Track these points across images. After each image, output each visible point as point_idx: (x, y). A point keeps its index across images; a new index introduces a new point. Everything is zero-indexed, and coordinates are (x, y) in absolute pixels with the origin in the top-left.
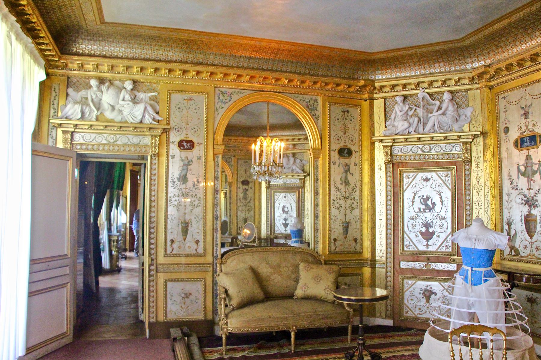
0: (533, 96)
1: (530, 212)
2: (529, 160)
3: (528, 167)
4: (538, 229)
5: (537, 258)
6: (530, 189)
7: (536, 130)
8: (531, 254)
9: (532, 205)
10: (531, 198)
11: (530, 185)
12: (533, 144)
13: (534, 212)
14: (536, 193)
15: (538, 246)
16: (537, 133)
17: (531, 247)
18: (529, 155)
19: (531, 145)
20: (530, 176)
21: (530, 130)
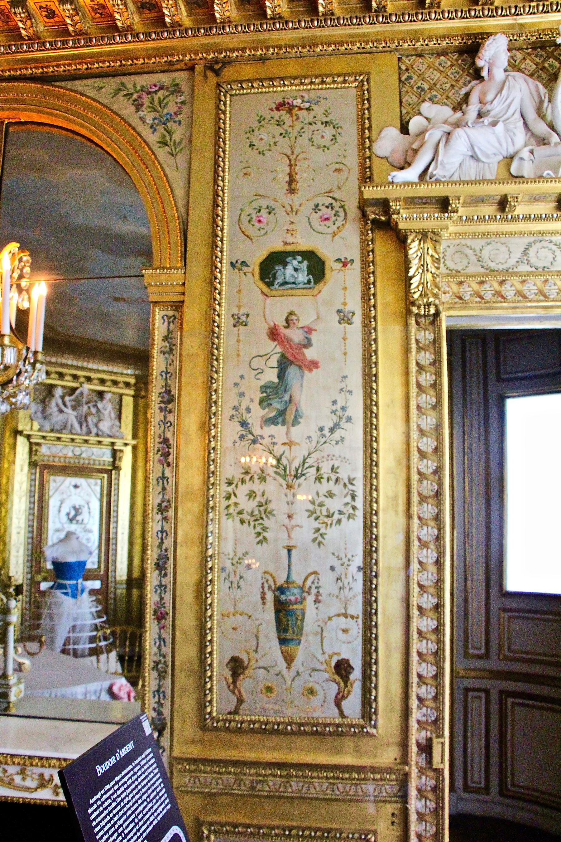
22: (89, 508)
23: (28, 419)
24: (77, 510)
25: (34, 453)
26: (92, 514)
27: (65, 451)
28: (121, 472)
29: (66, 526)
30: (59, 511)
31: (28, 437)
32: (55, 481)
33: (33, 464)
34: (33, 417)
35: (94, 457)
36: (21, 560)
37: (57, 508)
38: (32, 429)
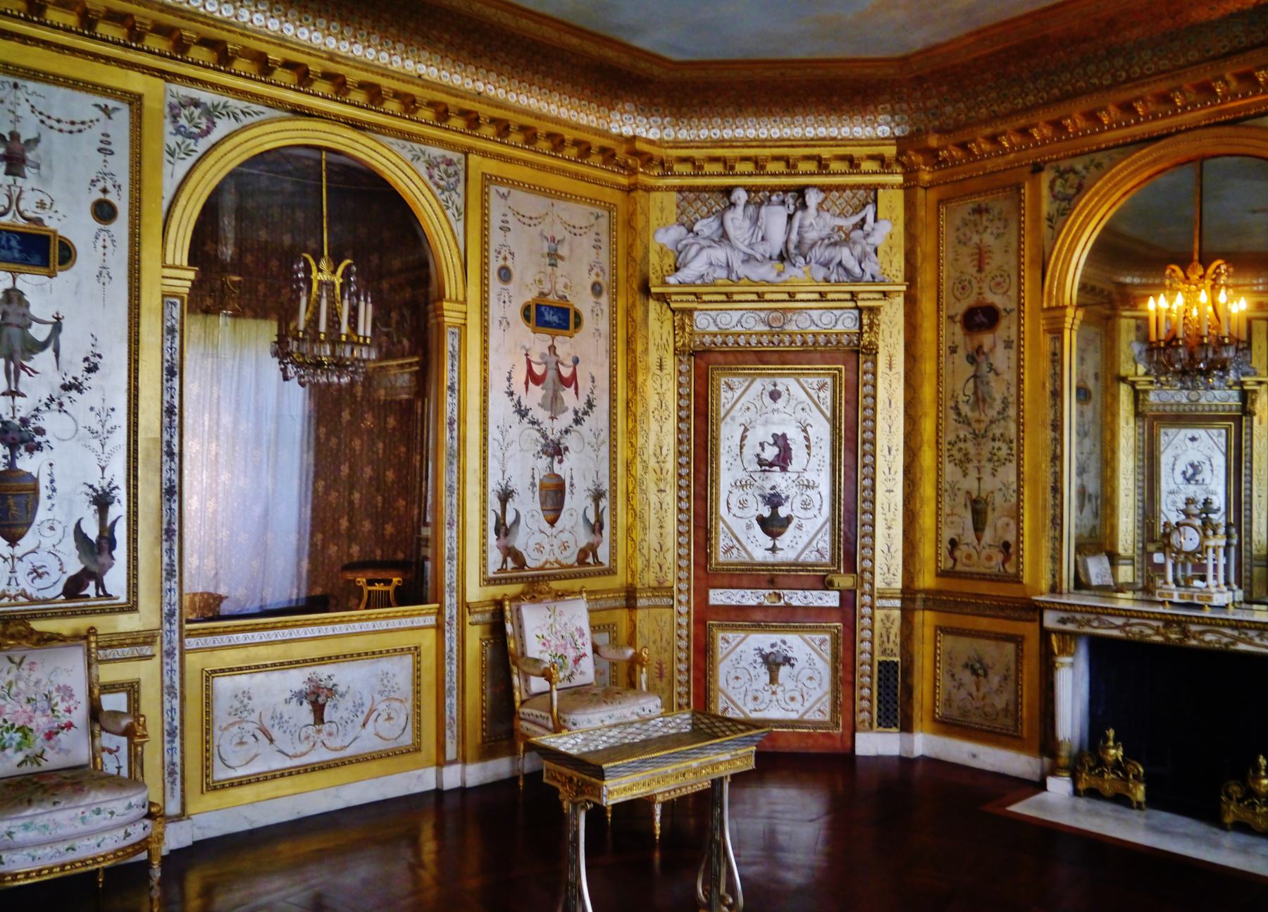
0: (44, 118)
1: (11, 464)
2: (15, 305)
3: (8, 324)
4: (41, 514)
5: (32, 601)
6: (13, 393)
7: (51, 224)
8: (13, 593)
9: (23, 441)
10: (17, 422)
11: (17, 380)
12: (37, 259)
13: (26, 463)
14: (37, 410)
15: (38, 564)
16: (54, 232)
17: (13, 571)
18: (14, 289)
19: (24, 262)
20: (18, 357)
21: (29, 214)
22: (1211, 465)
23: (1131, 363)
24: (1196, 468)
25: (1141, 402)
26: (1215, 472)
27: (1177, 398)
28: (1256, 419)
29: (1181, 487)
30: (1173, 469)
31: (1133, 384)
32: (1166, 434)
33: (1138, 414)
34: (1137, 359)
35: (1216, 402)
36: (1131, 527)
37: (1171, 466)
38: (1136, 374)
